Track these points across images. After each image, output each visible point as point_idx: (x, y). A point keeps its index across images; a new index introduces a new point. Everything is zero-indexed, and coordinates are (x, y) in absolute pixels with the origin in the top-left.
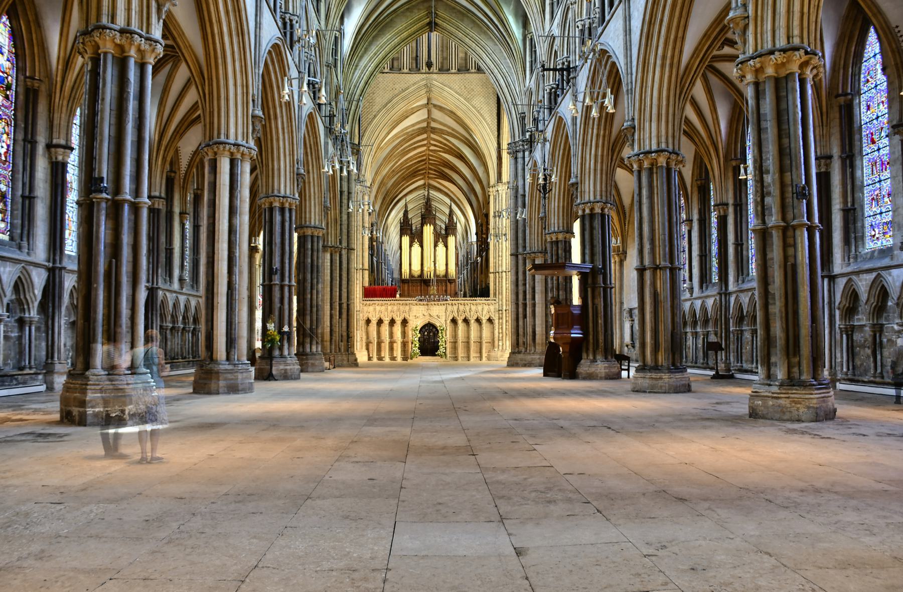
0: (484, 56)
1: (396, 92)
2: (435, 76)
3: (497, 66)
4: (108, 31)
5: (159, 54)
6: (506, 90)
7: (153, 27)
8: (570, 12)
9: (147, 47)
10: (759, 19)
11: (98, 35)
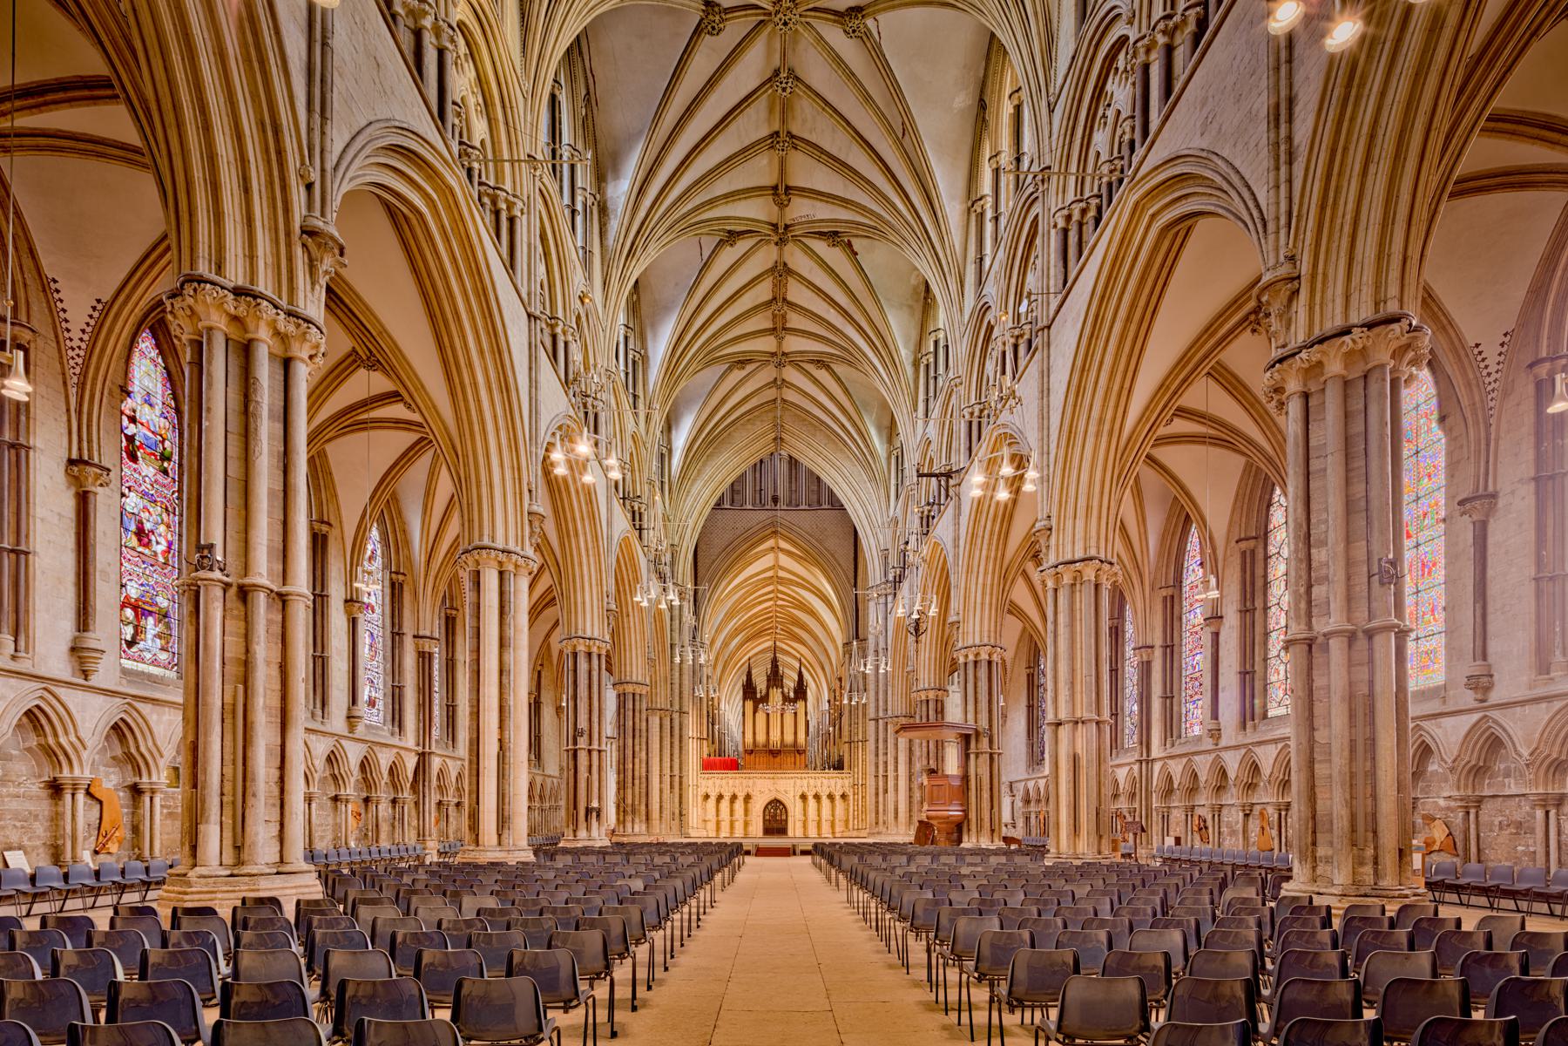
0: (840, 480)
1: (738, 533)
2: (779, 513)
3: (855, 492)
4: (208, 286)
5: (317, 346)
6: (865, 523)
7: (301, 295)
8: (954, 396)
9: (291, 328)
10: (1320, 277)
11: (192, 293)
